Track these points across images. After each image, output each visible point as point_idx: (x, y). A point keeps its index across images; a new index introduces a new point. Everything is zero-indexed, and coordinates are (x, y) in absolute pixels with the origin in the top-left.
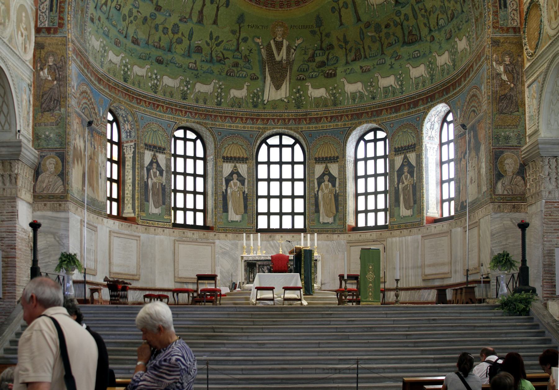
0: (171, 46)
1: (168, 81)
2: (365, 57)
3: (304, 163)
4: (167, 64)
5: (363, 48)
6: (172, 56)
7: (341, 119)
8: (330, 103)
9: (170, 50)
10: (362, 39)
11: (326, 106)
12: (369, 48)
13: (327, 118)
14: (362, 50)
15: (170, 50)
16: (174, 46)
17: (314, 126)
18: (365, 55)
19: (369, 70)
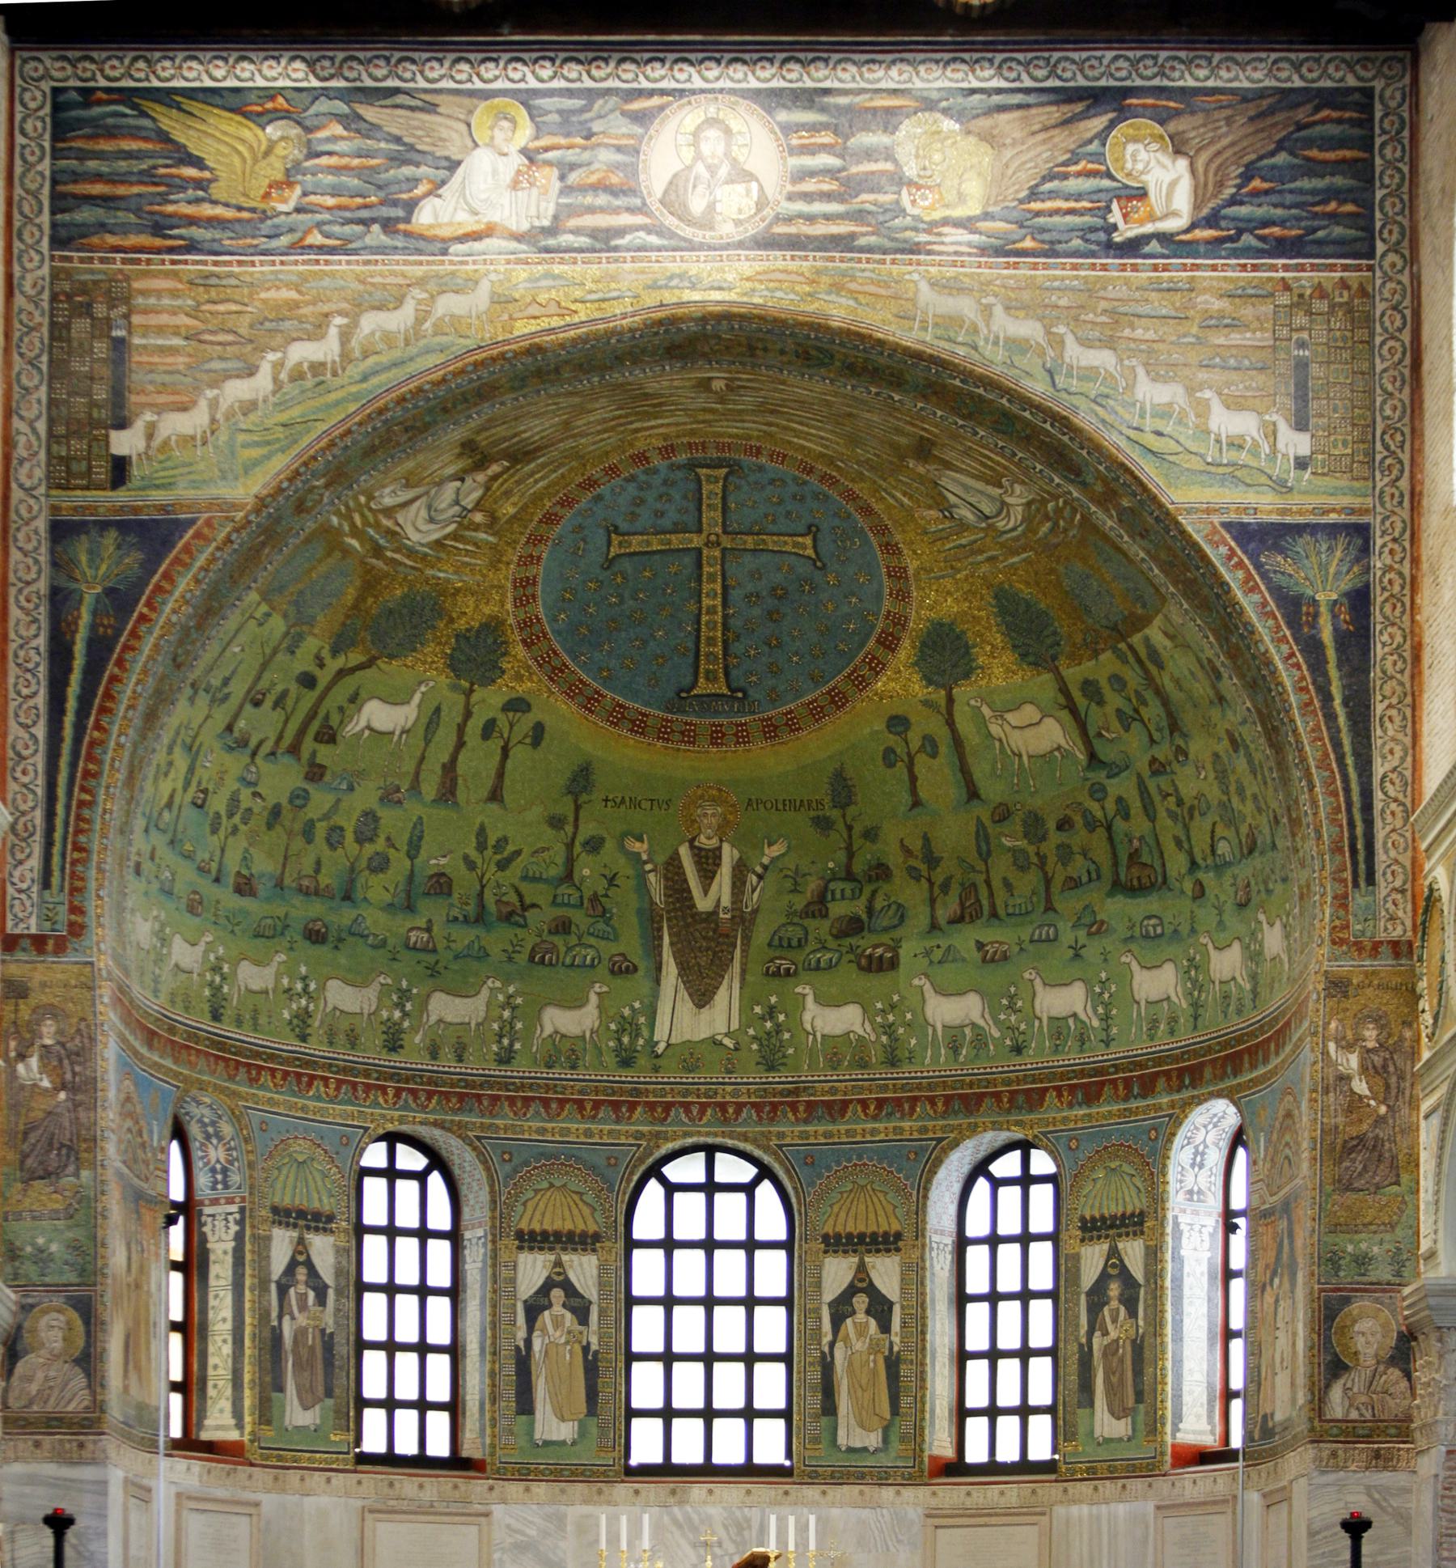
0: (352, 881)
1: (342, 997)
2: (994, 914)
3: (787, 1245)
4: (341, 940)
5: (988, 883)
6: (354, 913)
7: (912, 1110)
8: (875, 1056)
9: (347, 897)
10: (985, 856)
11: (864, 1065)
12: (1008, 885)
13: (864, 1103)
14: (983, 892)
15: (347, 897)
16: (361, 881)
17: (821, 1129)
18: (993, 906)
19: (1005, 957)
